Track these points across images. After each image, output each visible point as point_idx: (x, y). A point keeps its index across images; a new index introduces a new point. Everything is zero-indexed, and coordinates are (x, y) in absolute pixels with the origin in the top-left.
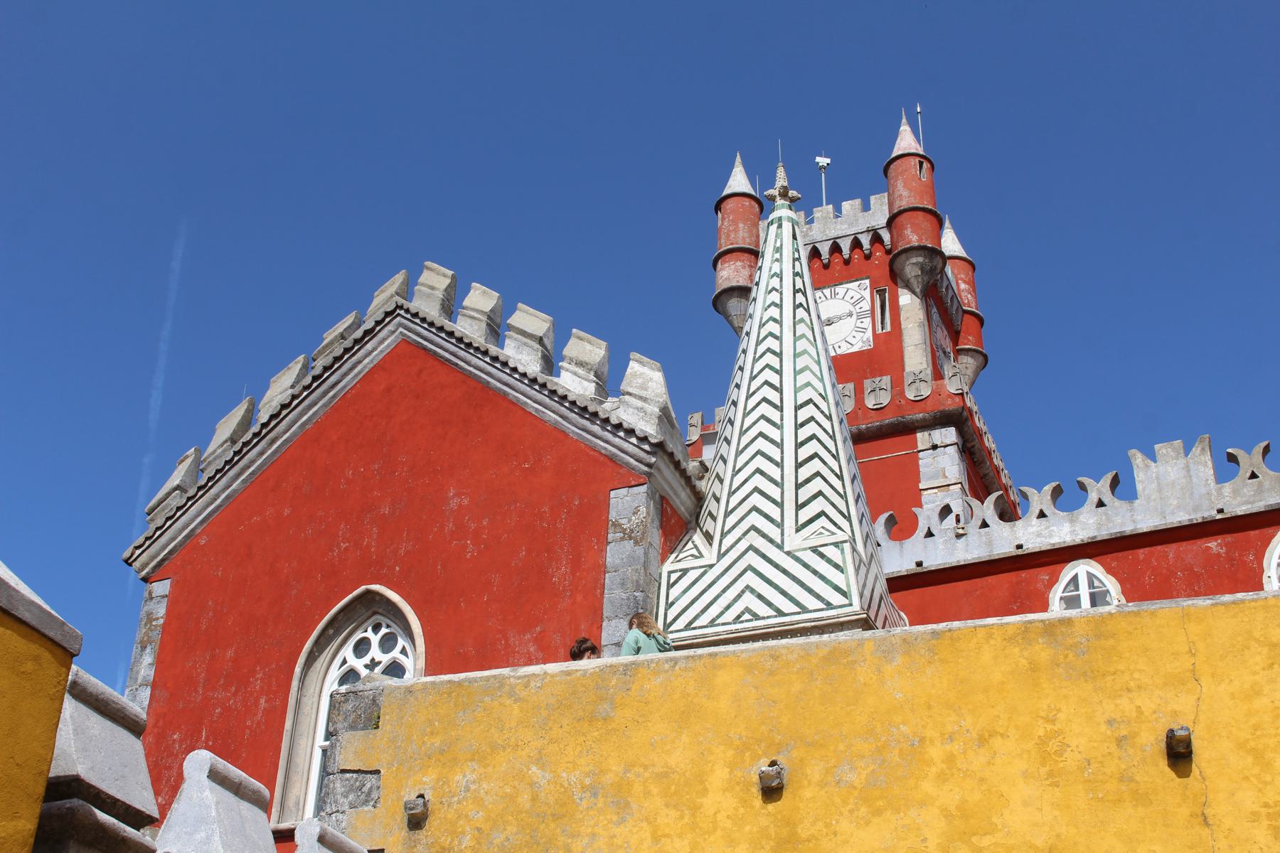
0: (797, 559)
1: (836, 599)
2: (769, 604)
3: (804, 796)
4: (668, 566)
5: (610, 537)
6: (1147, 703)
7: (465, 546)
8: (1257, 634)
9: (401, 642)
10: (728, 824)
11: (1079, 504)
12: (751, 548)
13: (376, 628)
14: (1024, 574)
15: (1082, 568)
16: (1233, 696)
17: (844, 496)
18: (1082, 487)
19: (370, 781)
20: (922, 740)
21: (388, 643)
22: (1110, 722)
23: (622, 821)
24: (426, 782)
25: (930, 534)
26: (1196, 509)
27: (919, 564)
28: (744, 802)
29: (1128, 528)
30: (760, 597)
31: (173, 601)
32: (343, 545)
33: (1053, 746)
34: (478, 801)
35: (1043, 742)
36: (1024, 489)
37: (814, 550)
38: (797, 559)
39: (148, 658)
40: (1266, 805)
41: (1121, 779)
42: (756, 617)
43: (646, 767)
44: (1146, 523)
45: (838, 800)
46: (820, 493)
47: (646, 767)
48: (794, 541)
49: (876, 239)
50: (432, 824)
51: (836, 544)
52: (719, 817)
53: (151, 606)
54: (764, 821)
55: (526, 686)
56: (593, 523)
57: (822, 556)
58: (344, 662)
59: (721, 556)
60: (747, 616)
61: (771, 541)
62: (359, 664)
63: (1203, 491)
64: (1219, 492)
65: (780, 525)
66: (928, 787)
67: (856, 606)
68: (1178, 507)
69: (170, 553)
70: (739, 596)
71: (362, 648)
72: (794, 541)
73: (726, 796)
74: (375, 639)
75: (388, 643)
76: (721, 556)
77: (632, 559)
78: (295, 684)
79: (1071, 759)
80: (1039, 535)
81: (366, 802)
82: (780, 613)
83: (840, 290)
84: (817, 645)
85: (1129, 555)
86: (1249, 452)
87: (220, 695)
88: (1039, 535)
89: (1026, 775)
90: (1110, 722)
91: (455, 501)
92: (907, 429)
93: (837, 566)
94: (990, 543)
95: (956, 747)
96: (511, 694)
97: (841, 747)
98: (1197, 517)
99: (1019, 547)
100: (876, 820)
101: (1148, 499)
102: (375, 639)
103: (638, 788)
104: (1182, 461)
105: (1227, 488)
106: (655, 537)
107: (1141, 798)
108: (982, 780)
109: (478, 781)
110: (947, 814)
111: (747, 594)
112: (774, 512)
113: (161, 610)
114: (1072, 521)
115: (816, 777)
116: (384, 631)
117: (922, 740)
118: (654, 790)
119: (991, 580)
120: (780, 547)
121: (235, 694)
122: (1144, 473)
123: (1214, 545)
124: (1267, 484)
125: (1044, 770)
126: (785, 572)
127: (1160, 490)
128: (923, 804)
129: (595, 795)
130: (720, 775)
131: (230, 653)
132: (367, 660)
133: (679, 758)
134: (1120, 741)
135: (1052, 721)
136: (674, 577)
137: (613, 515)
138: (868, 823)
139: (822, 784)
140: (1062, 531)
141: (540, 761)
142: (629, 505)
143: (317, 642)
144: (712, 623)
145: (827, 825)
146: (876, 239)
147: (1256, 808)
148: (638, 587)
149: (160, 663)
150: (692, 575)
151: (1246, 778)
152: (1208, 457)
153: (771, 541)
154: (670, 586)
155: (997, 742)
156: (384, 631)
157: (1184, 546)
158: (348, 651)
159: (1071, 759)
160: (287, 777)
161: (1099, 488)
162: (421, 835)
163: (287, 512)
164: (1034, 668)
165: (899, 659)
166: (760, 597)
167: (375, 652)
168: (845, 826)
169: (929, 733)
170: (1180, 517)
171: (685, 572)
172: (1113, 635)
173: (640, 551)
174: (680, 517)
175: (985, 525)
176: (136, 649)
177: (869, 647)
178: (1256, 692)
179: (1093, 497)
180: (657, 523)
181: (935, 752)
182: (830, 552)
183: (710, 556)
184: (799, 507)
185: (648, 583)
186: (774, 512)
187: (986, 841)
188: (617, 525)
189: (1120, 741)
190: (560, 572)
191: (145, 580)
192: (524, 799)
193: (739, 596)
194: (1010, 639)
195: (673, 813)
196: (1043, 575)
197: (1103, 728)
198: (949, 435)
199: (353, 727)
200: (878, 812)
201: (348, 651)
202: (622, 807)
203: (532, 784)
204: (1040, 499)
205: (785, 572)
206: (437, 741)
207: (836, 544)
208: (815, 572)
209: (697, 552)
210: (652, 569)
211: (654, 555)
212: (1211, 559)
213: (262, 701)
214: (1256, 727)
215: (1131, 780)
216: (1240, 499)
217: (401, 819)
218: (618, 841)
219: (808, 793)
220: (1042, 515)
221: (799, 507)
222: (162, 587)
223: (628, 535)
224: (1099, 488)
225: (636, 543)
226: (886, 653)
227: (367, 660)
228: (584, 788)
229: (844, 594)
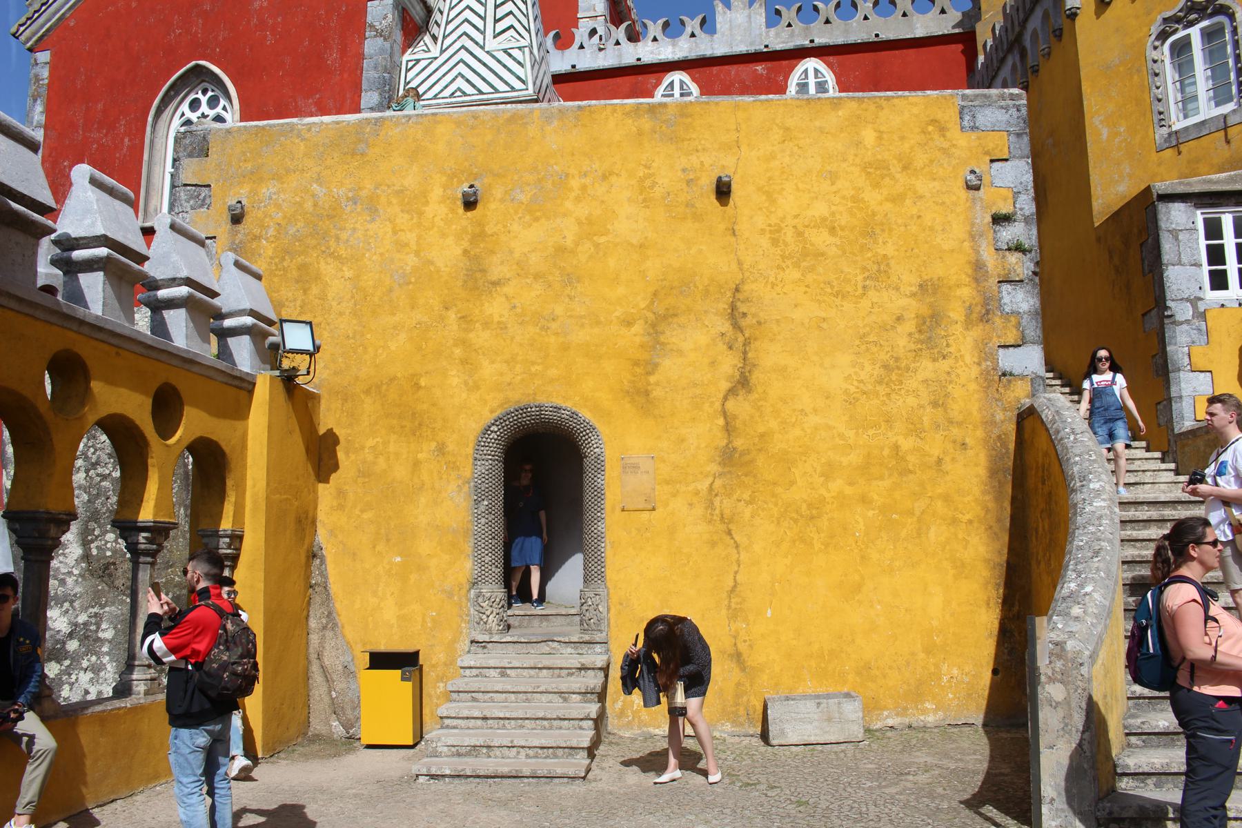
0: (494, 57)
1: (518, 85)
2: (474, 86)
3: (489, 209)
4: (406, 57)
5: (367, 34)
6: (707, 159)
7: (266, 36)
8: (778, 121)
9: (223, 102)
10: (442, 224)
11: (680, 34)
12: (463, 47)
13: (205, 92)
14: (640, 78)
15: (677, 77)
16: (758, 159)
17: (527, 16)
18: (682, 23)
19: (204, 192)
20: (567, 175)
21: (213, 103)
22: (684, 170)
23: (373, 220)
24: (242, 193)
25: (582, 47)
26: (751, 44)
27: (574, 67)
28: (452, 211)
29: (708, 53)
30: (468, 81)
31: (54, 66)
32: (178, 32)
33: (648, 183)
34: (278, 206)
35: (642, 180)
36: (646, 21)
37: (505, 51)
38: (494, 57)
39: (39, 108)
40: (770, 225)
41: (687, 206)
42: (465, 94)
43: (389, 186)
44: (720, 50)
45: (512, 211)
46: (511, 13)
47: (389, 186)
48: (491, 44)
50: (247, 220)
51: (520, 48)
52: (436, 219)
53: (37, 69)
54: (464, 223)
55: (309, 130)
57: (510, 55)
58: (183, 114)
59: (442, 51)
60: (458, 93)
61: (477, 43)
62: (193, 117)
63: (758, 32)
64: (767, 33)
65: (483, 33)
66: (569, 205)
67: (531, 91)
68: (741, 41)
69: (48, 30)
70: (454, 80)
71: (195, 105)
72: (491, 44)
73: (440, 205)
74: (204, 100)
75: (213, 103)
76: (442, 51)
77: (382, 51)
78: (149, 129)
79: (658, 192)
80: (652, 53)
81: (202, 206)
82: (481, 93)
84: (503, 111)
85: (707, 70)
86: (789, 9)
87: (95, 135)
88: (652, 53)
89: (629, 200)
90: (684, 170)
93: (519, 63)
94: (620, 56)
95: (587, 181)
96: (299, 136)
97: (516, 178)
98: (752, 49)
99: (639, 59)
100: (535, 224)
101: (723, 34)
102: (204, 100)
103: (383, 199)
104: (746, 12)
105: (773, 31)
106: (398, 36)
107: (697, 217)
108: (603, 202)
109: (278, 193)
110: (580, 223)
111: (459, 78)
112: (480, 23)
113: (45, 73)
114: (674, 45)
115: (499, 196)
116: (210, 94)
117: (567, 175)
118: (394, 201)
119: (619, 80)
120: (482, 48)
121: (106, 135)
122: (723, 18)
123: (760, 68)
124: (797, 32)
125: (641, 198)
126: (485, 65)
127: (731, 29)
128: (565, 215)
129: (355, 203)
130: (437, 193)
131: (100, 106)
132: (199, 113)
133: (411, 181)
134: (689, 182)
135: (646, 167)
136: (410, 64)
137: (369, 19)
138: (530, 226)
139: (502, 200)
140: (667, 51)
141: (319, 180)
143: (163, 100)
144: (435, 97)
145: (505, 226)
147: (763, 227)
148: (386, 70)
149: (48, 111)
150: (423, 64)
151: (760, 209)
152: (763, 10)
153: (477, 43)
154: (408, 70)
155: (613, 179)
156: (210, 94)
157: (741, 67)
158: (185, 107)
159: (658, 192)
160: (147, 192)
161: (692, 25)
162: (240, 227)
163: (134, 5)
164: (640, 133)
165: (556, 123)
166: (468, 81)
167: (204, 108)
168: (515, 227)
169: (572, 171)
170: (741, 48)
171: (418, 61)
172: (691, 116)
173: (387, 45)
174: (415, 24)
175: (618, 43)
176: (29, 101)
177: (537, 114)
178: (773, 157)
179: (689, 30)
180: (399, 26)
181: (575, 183)
182: (515, 53)
183: (435, 51)
184: (496, 21)
185: (393, 68)
186: (480, 23)
187: (602, 240)
188: (372, 26)
189: (689, 182)
190: (333, 57)
191: (31, 50)
192: (309, 205)
193: (454, 80)
194: (627, 114)
195: (406, 216)
196: (652, 79)
197: (679, 173)
199: (190, 155)
200: (537, 219)
201: (185, 107)
202: (373, 210)
203: (313, 196)
204: (655, 29)
205: (485, 65)
206: (249, 166)
207: (520, 48)
208: (505, 66)
209: (425, 48)
210: (396, 58)
211: (397, 48)
212: (756, 77)
213: (126, 140)
214: (770, 179)
215: (693, 206)
216: (779, 40)
217: (226, 217)
218: (371, 233)
219: (493, 206)
220: (655, 39)
221: (496, 21)
222: (44, 57)
223: (380, 34)
224: (692, 25)
225: (385, 39)
226: (548, 119)
227: (199, 113)
228: (348, 199)
229: (523, 82)
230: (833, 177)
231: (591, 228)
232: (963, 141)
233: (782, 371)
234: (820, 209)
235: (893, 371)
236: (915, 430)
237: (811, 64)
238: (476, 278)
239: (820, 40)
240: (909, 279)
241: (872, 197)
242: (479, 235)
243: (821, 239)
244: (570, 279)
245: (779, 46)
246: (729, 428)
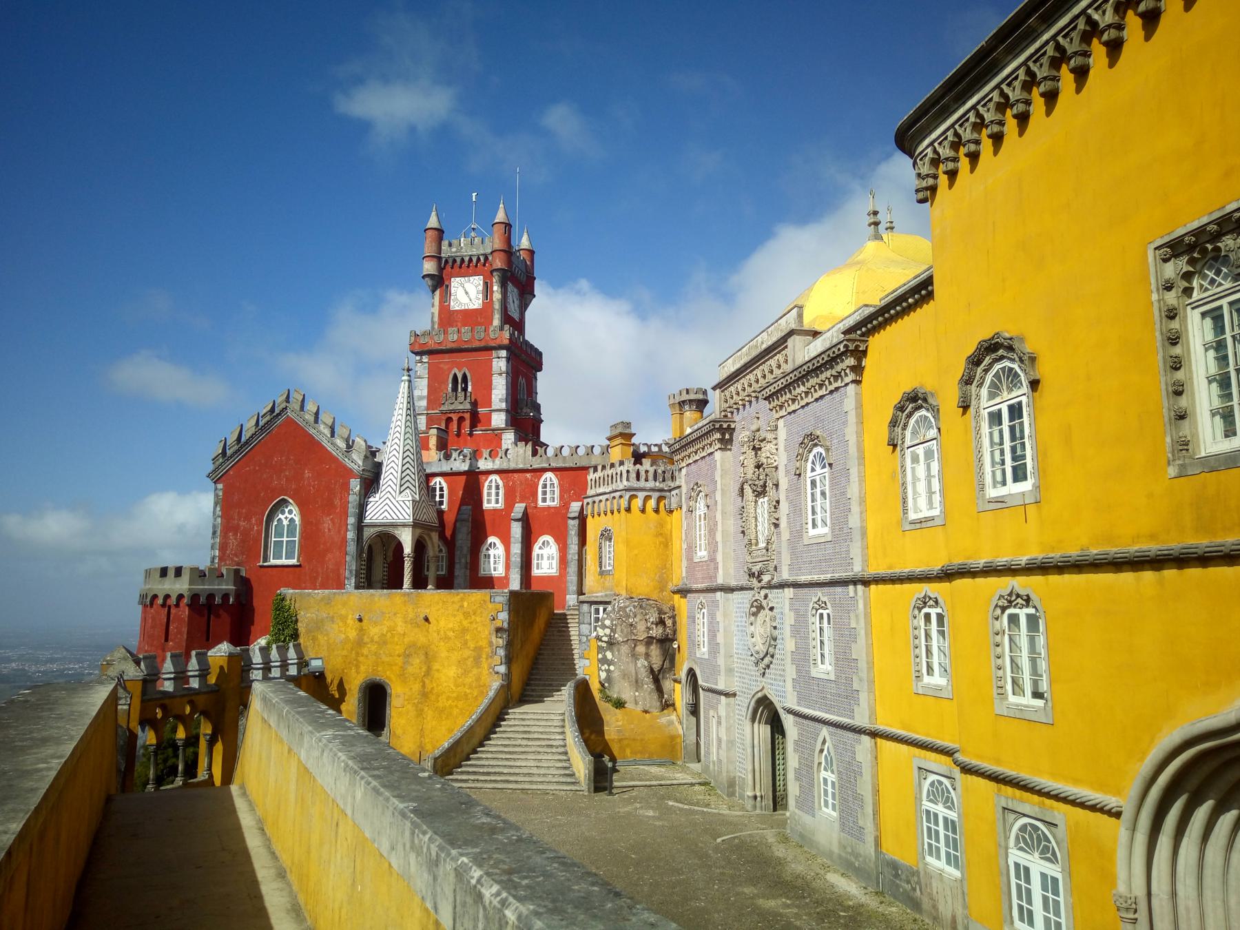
3: (365, 621)
21: (290, 512)
44: (513, 466)
49: (486, 259)
56: (346, 487)
71: (283, 513)
83: (472, 278)
91: (307, 474)
92: (489, 349)
123: (528, 475)
133: (343, 612)
142: (355, 485)
146: (486, 259)
170: (521, 466)
185: (362, 508)
190: (337, 502)
198: (504, 353)
212: (527, 479)
230: (455, 616)
231: (391, 629)
232: (490, 606)
233: (438, 670)
234: (451, 625)
235: (466, 672)
236: (470, 687)
237: (549, 475)
238: (360, 643)
239: (554, 465)
240: (472, 645)
241: (465, 623)
242: (361, 630)
243: (451, 634)
244: (385, 643)
245: (535, 466)
246: (424, 686)
